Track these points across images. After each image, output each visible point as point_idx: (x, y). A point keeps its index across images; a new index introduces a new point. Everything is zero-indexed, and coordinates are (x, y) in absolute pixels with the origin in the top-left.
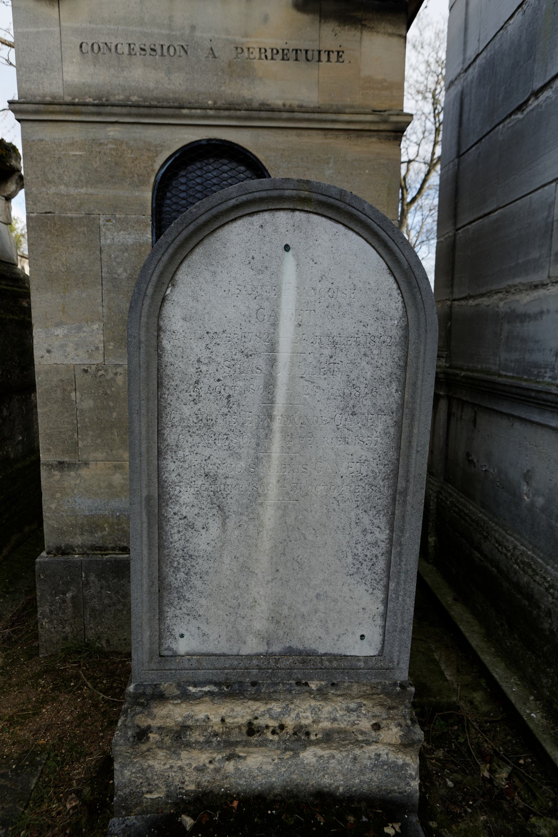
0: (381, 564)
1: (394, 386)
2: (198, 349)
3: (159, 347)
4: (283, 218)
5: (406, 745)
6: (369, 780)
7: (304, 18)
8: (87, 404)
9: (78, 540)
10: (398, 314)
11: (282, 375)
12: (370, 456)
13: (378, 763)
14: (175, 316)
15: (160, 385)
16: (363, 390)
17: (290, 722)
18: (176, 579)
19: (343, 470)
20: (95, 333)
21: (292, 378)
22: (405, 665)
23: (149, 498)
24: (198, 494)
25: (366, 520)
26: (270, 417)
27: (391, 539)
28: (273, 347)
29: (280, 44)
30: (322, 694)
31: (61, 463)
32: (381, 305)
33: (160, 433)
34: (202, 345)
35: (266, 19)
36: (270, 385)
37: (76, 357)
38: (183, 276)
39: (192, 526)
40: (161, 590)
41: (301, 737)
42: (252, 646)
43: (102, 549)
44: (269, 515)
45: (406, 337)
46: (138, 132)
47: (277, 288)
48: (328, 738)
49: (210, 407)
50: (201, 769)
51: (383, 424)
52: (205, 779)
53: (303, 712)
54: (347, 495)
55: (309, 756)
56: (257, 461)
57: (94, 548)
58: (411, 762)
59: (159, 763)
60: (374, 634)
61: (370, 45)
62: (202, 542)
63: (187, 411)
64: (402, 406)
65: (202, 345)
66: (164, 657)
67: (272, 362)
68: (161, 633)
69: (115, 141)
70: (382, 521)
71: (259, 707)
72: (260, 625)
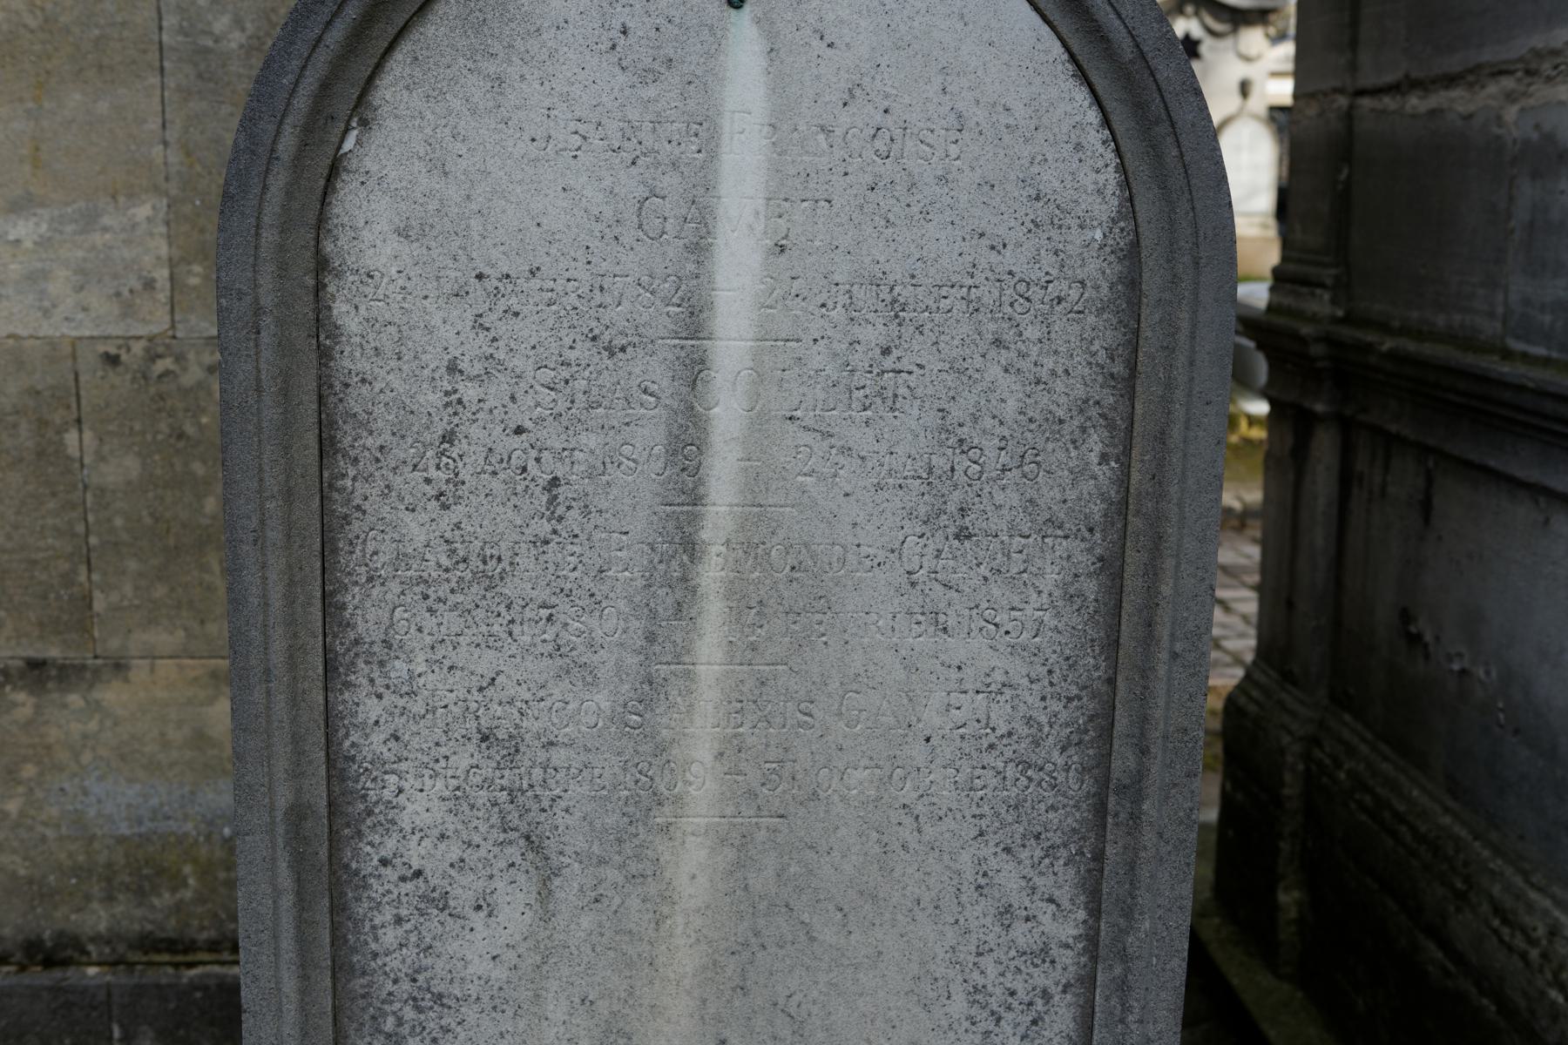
1: (1095, 443)
2: (449, 330)
3: (321, 326)
8: (120, 469)
9: (97, 919)
10: (1105, 208)
11: (727, 413)
12: (1018, 669)
14: (375, 221)
15: (327, 447)
16: (993, 458)
19: (932, 718)
20: (141, 234)
21: (758, 421)
23: (298, 813)
24: (457, 798)
25: (1010, 879)
26: (691, 548)
27: (1091, 940)
28: (694, 322)
31: (36, 666)
32: (1049, 180)
33: (330, 605)
34: (461, 316)
36: (687, 444)
38: (388, 91)
39: (442, 902)
44: (692, 865)
45: (1131, 283)
47: (705, 129)
49: (493, 517)
51: (1059, 565)
54: (947, 796)
56: (650, 690)
57: (150, 944)
62: (476, 952)
63: (416, 530)
64: (1121, 507)
65: (461, 316)
67: (694, 370)
70: (1063, 881)
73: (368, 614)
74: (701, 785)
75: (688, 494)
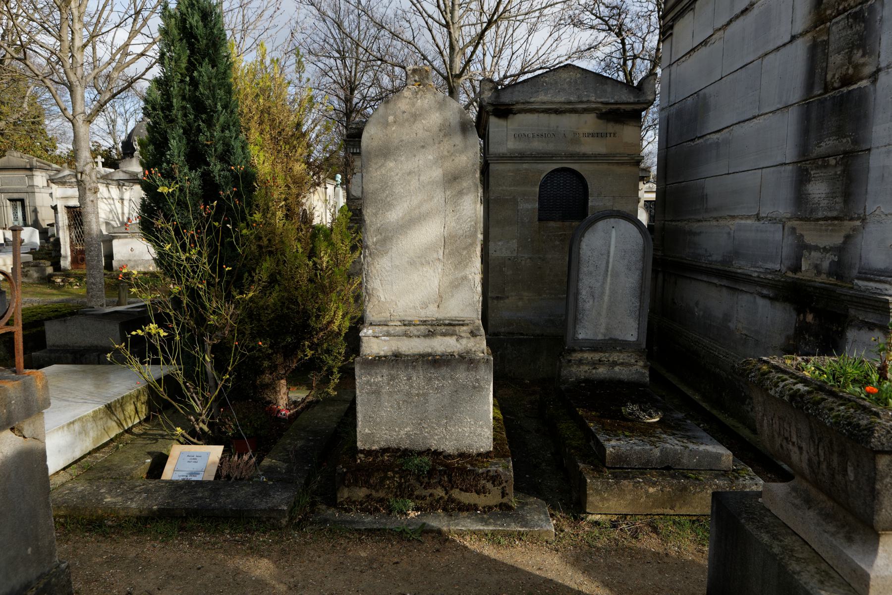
0: (637, 313)
2: (589, 253)
3: (579, 253)
4: (612, 220)
5: (645, 367)
6: (635, 377)
7: (601, 121)
8: (510, 272)
9: (503, 330)
11: (611, 260)
13: (637, 372)
14: (584, 245)
17: (611, 359)
18: (580, 316)
20: (514, 244)
22: (645, 343)
28: (609, 252)
29: (591, 131)
30: (620, 351)
35: (586, 123)
36: (608, 262)
37: (506, 254)
40: (576, 320)
41: (615, 364)
42: (600, 337)
43: (513, 334)
44: (606, 298)
45: (644, 250)
46: (535, 166)
47: (610, 237)
48: (622, 364)
50: (586, 372)
51: (638, 273)
52: (587, 375)
53: (615, 357)
55: (617, 369)
56: (603, 283)
57: (509, 333)
58: (646, 372)
59: (574, 369)
60: (635, 333)
61: (627, 132)
62: (588, 306)
66: (576, 340)
67: (609, 256)
68: (575, 332)
69: (526, 169)
70: (638, 300)
71: (602, 354)
72: (602, 331)
73: (581, 277)
74: (607, 292)
75: (607, 267)
